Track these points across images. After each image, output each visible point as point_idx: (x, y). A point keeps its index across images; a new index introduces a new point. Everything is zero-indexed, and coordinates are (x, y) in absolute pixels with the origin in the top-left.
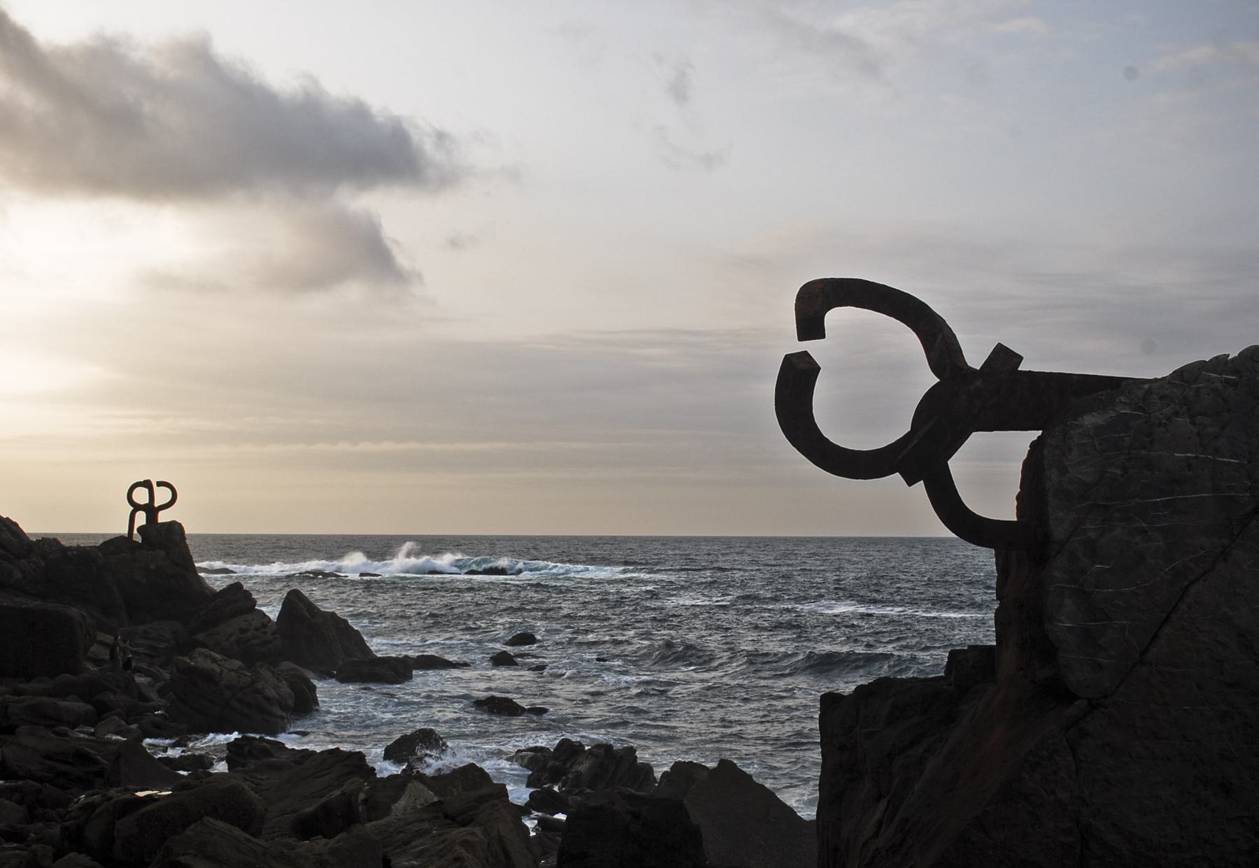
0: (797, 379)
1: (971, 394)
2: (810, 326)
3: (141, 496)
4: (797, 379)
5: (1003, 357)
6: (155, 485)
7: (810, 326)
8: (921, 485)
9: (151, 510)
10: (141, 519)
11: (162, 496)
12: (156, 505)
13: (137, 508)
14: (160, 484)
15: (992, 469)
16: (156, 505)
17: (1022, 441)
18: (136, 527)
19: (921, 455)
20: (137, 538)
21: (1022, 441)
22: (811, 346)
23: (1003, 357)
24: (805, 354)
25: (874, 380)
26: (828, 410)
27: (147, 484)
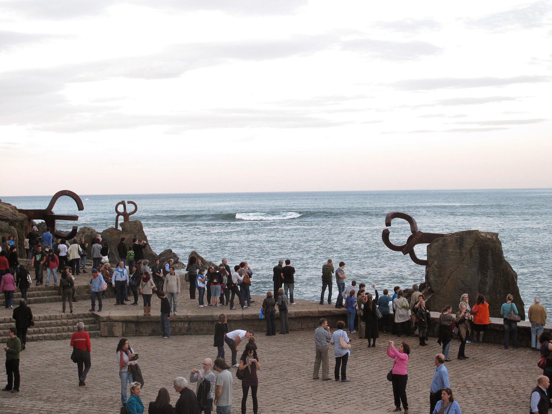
0: (385, 235)
1: (417, 237)
2: (388, 224)
3: (121, 209)
4: (385, 235)
6: (126, 204)
7: (388, 224)
8: (408, 254)
9: (126, 215)
10: (121, 219)
11: (130, 208)
12: (128, 211)
13: (119, 214)
14: (129, 202)
16: (128, 211)
17: (426, 245)
18: (119, 222)
20: (120, 228)
24: (387, 230)
26: (393, 239)
27: (123, 203)
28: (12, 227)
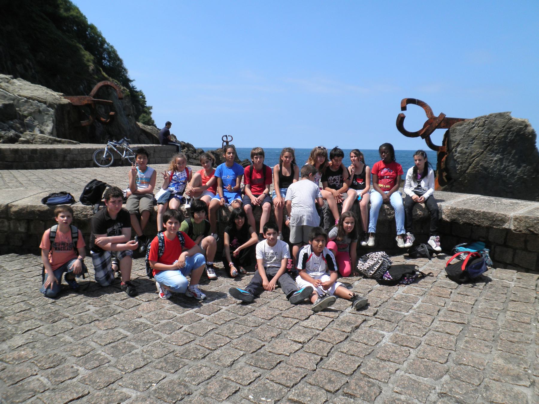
2: (404, 108)
3: (225, 139)
5: (442, 114)
7: (404, 108)
9: (227, 142)
10: (225, 144)
11: (229, 139)
13: (224, 141)
15: (438, 137)
17: (444, 131)
19: (425, 134)
21: (444, 131)
22: (404, 112)
23: (442, 114)
24: (403, 114)
25: (416, 119)
27: (226, 136)
28: (50, 109)
